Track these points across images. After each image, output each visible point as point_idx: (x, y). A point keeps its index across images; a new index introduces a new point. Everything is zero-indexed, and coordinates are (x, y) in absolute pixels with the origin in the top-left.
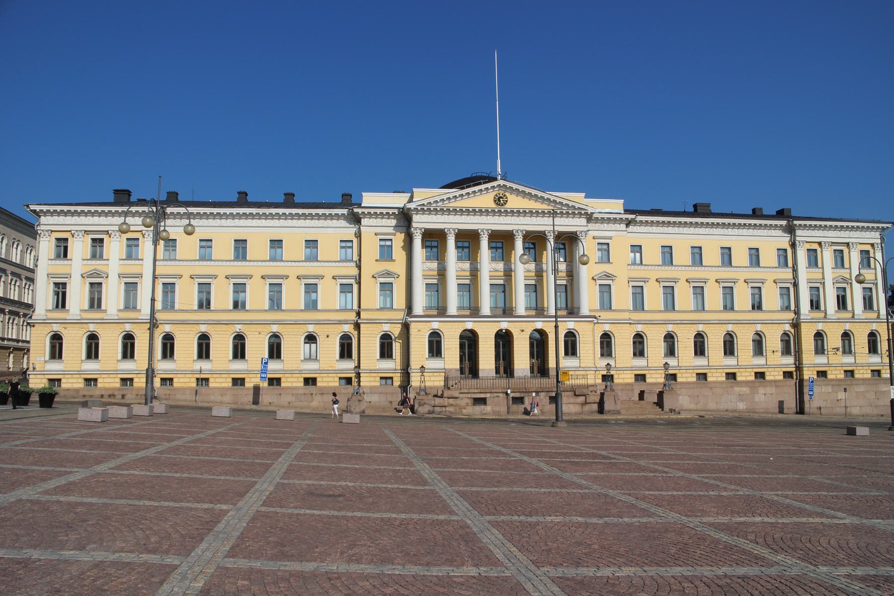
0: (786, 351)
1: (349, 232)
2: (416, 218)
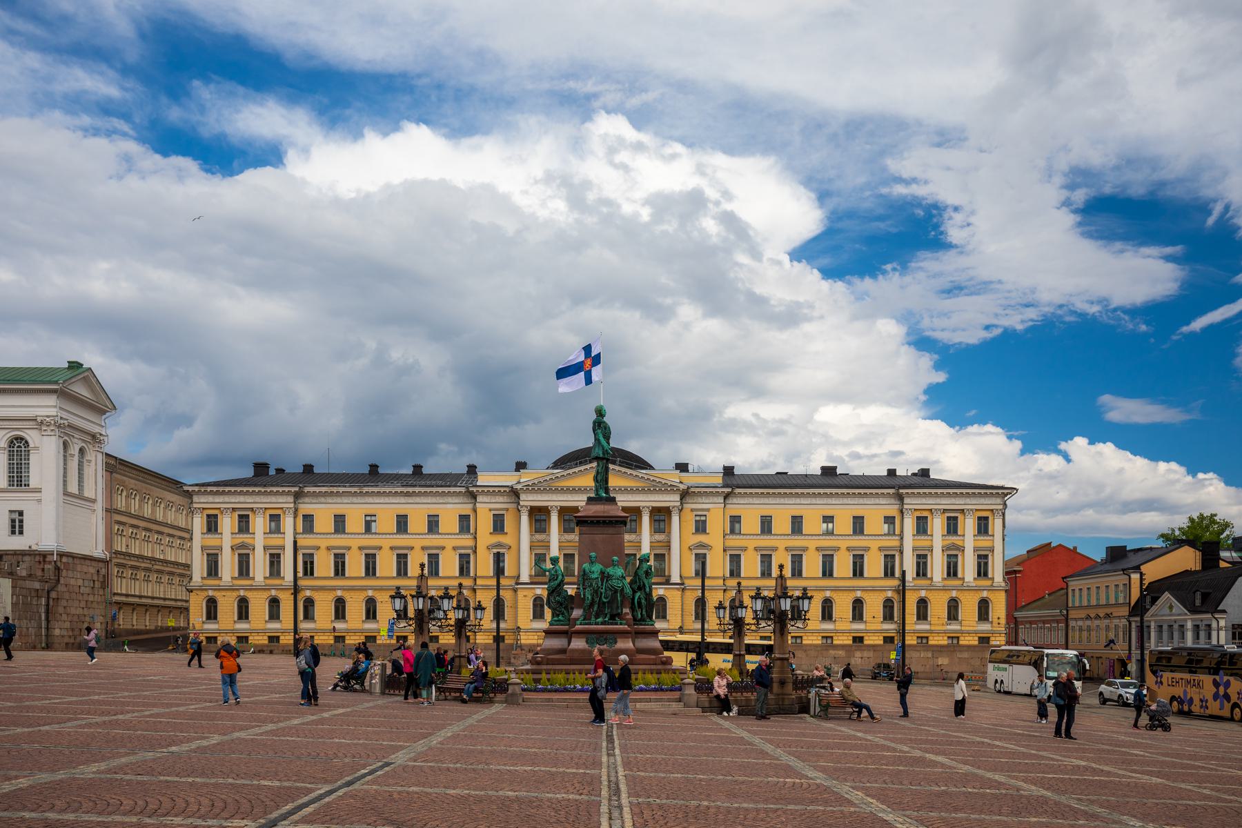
0: (888, 616)
1: (466, 509)
2: (523, 497)
